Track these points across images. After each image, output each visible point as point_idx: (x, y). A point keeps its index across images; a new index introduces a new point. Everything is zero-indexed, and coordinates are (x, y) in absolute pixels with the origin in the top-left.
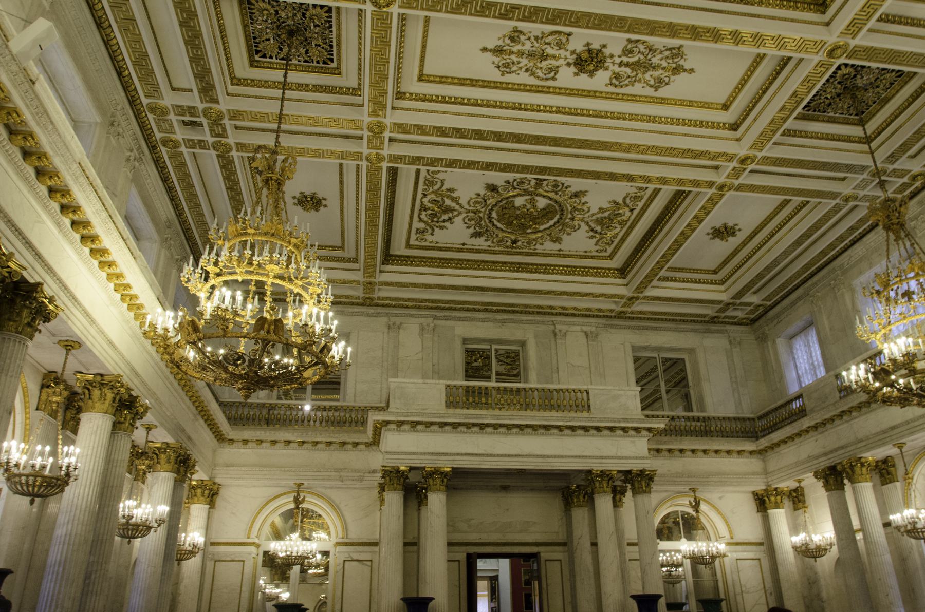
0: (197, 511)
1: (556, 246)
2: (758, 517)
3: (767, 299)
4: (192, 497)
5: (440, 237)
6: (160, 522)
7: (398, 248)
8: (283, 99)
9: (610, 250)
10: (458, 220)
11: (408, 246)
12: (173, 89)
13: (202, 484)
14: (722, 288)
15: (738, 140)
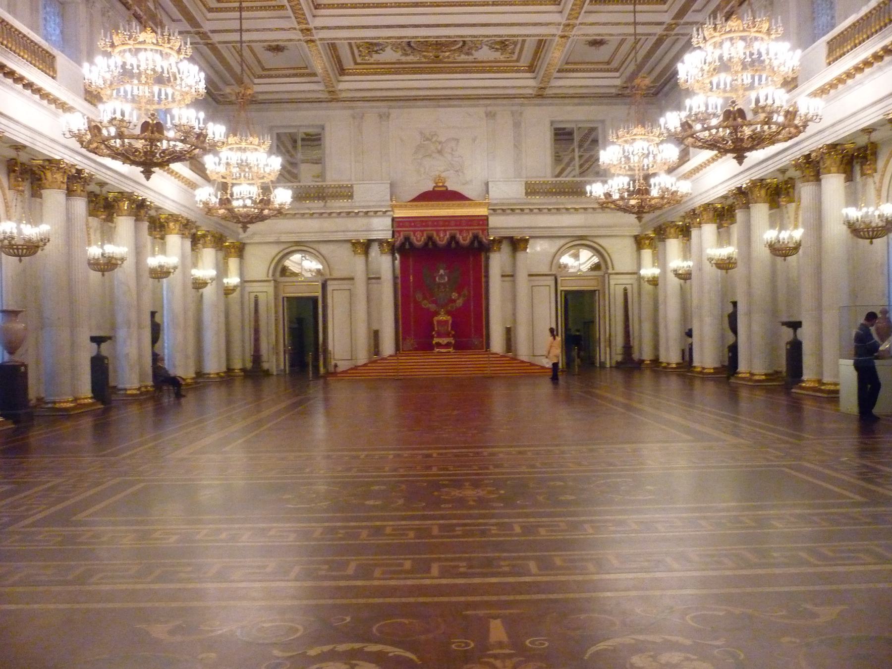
0: (233, 263)
1: (470, 58)
2: (635, 255)
3: (655, 80)
4: (227, 256)
5: (376, 57)
6: (212, 279)
7: (348, 64)
8: (241, 19)
9: (515, 57)
10: (388, 49)
11: (356, 63)
12: (173, 21)
13: (233, 245)
14: (617, 74)
15: (561, 12)
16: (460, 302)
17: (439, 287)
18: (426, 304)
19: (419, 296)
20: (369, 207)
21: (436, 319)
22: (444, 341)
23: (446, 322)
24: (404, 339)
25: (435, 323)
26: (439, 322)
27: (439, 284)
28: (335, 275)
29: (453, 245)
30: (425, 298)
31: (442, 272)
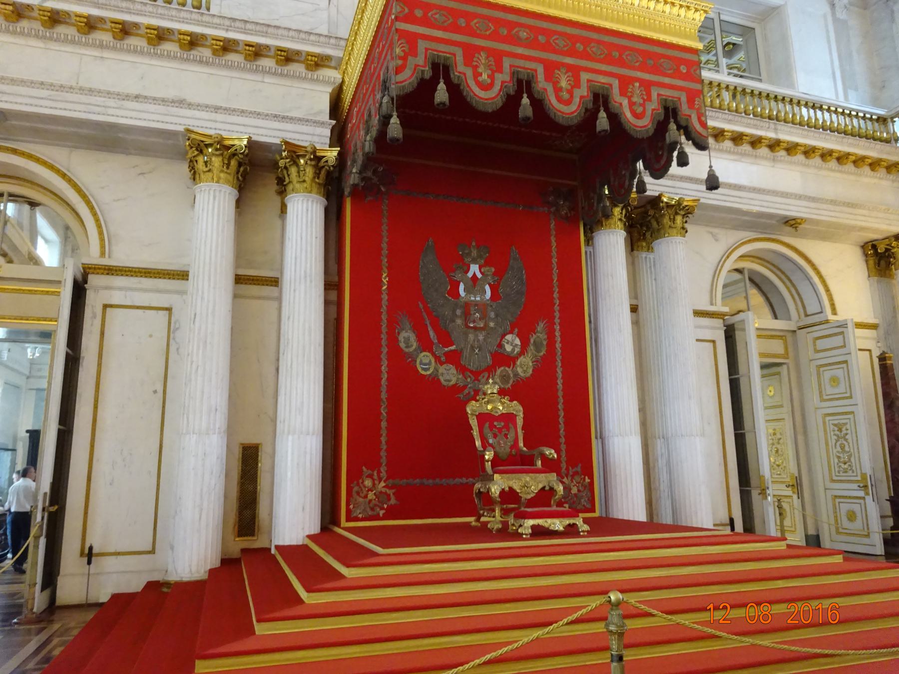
16: (525, 366)
17: (467, 314)
18: (425, 364)
19: (407, 338)
20: (266, 28)
21: (472, 408)
22: (529, 484)
23: (509, 418)
24: (354, 476)
25: (474, 422)
26: (483, 418)
27: (467, 306)
28: (120, 257)
29: (603, 122)
30: (426, 345)
31: (474, 269)
